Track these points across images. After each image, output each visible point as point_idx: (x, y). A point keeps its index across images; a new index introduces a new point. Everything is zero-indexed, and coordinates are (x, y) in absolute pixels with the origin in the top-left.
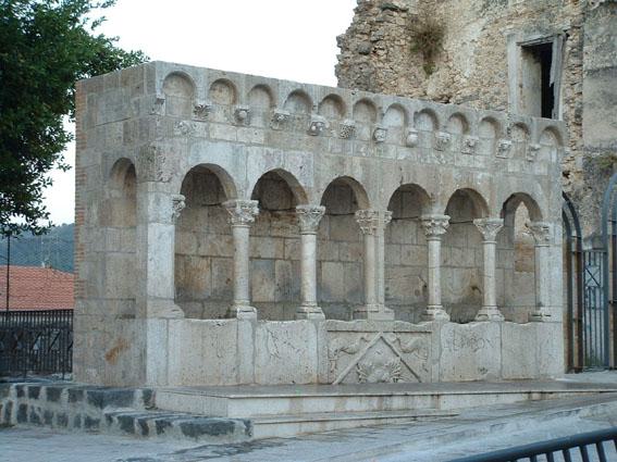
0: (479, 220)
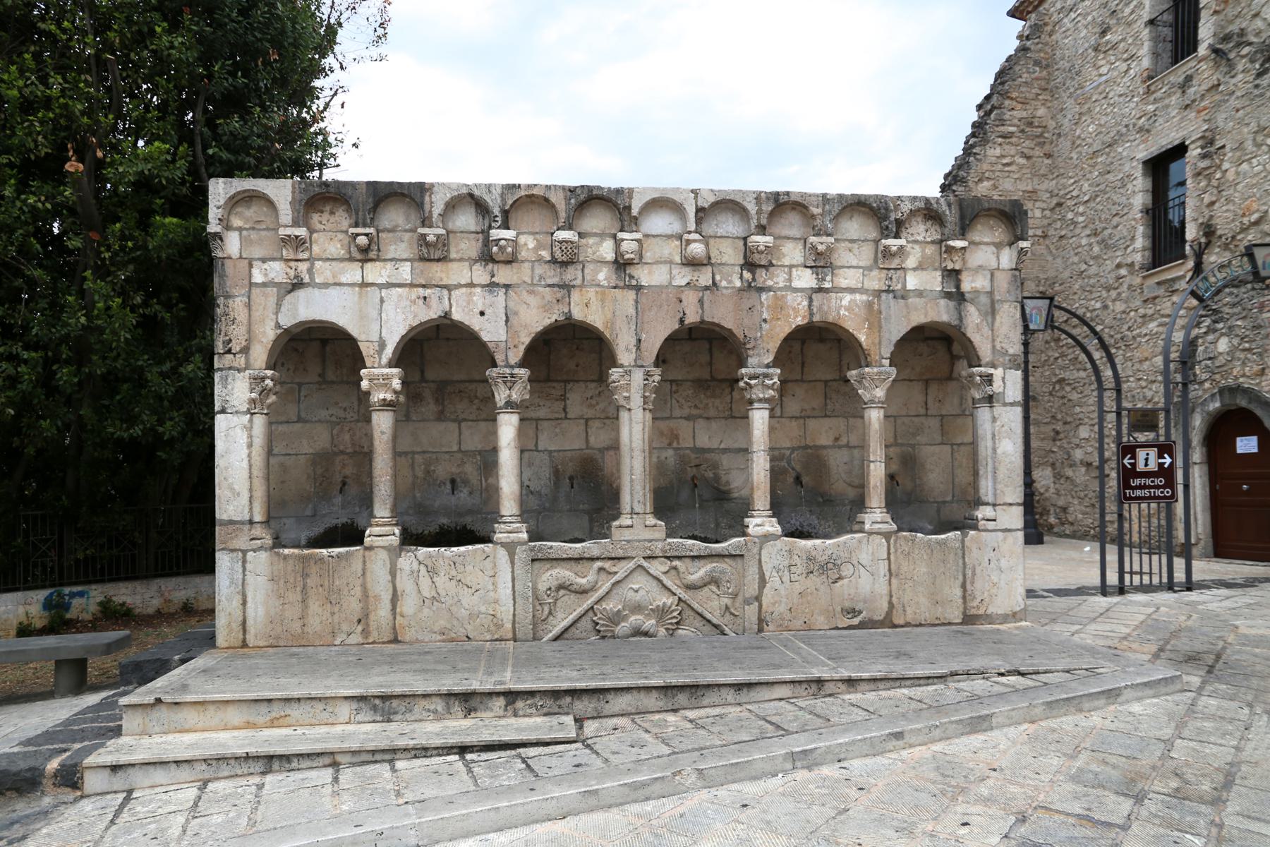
0: (854, 372)
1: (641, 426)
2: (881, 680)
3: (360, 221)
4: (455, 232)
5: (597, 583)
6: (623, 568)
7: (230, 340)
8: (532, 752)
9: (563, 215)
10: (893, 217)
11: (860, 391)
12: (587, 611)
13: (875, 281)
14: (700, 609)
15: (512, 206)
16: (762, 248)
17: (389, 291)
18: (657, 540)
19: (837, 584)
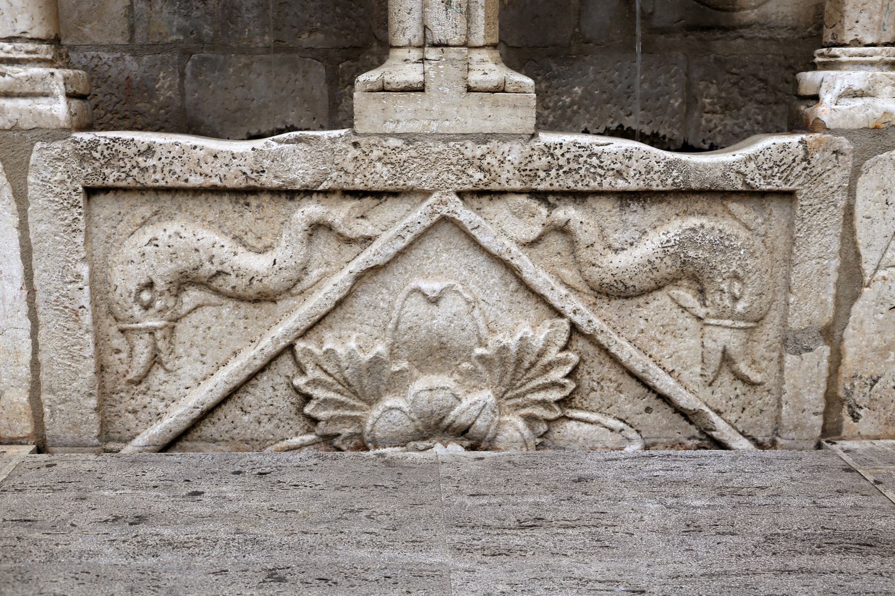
5: (304, 269)
12: (274, 358)
18: (505, 137)
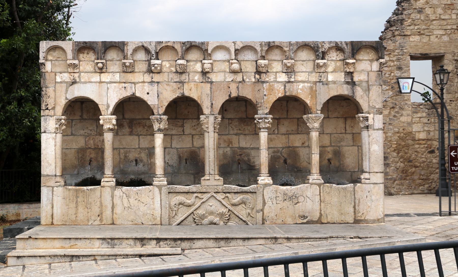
0: (305, 116)
1: (213, 139)
2: (301, 238)
3: (99, 57)
4: (137, 61)
5: (195, 202)
6: (206, 196)
7: (48, 104)
8: (165, 257)
9: (180, 54)
10: (321, 50)
11: (308, 124)
12: (191, 214)
13: (314, 77)
14: (238, 214)
15: (159, 50)
16: (263, 65)
17: (111, 84)
19: (297, 205)
